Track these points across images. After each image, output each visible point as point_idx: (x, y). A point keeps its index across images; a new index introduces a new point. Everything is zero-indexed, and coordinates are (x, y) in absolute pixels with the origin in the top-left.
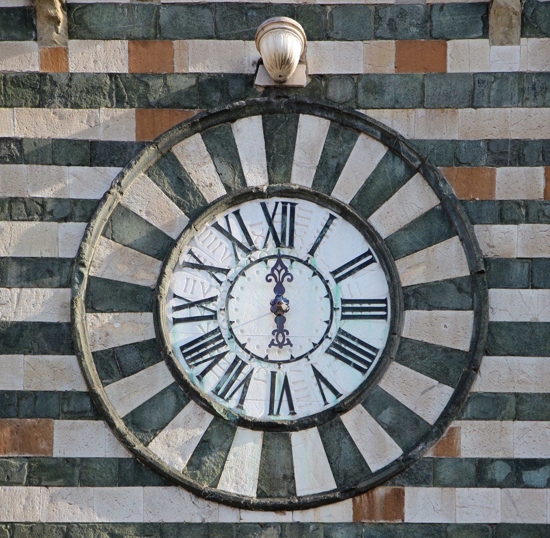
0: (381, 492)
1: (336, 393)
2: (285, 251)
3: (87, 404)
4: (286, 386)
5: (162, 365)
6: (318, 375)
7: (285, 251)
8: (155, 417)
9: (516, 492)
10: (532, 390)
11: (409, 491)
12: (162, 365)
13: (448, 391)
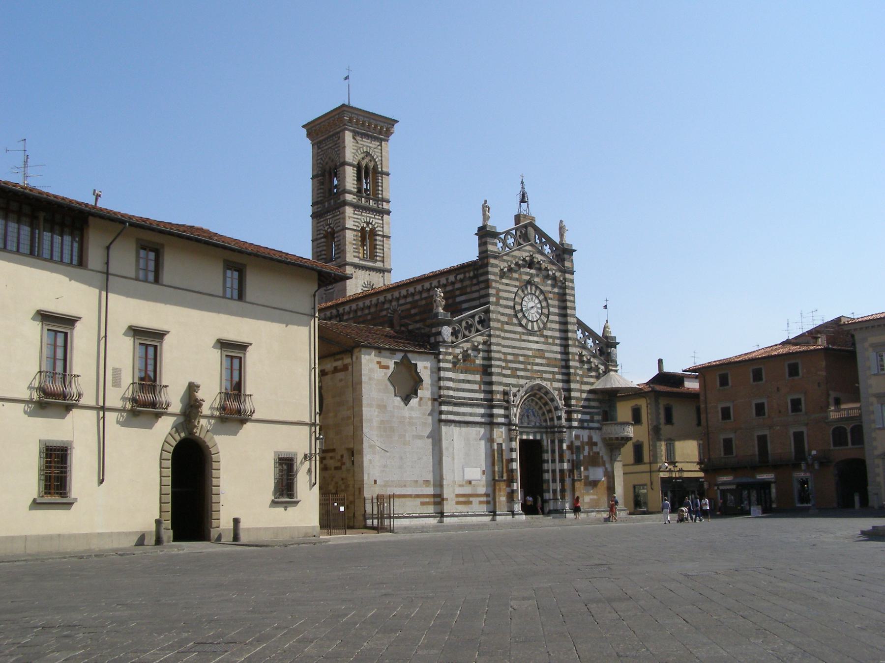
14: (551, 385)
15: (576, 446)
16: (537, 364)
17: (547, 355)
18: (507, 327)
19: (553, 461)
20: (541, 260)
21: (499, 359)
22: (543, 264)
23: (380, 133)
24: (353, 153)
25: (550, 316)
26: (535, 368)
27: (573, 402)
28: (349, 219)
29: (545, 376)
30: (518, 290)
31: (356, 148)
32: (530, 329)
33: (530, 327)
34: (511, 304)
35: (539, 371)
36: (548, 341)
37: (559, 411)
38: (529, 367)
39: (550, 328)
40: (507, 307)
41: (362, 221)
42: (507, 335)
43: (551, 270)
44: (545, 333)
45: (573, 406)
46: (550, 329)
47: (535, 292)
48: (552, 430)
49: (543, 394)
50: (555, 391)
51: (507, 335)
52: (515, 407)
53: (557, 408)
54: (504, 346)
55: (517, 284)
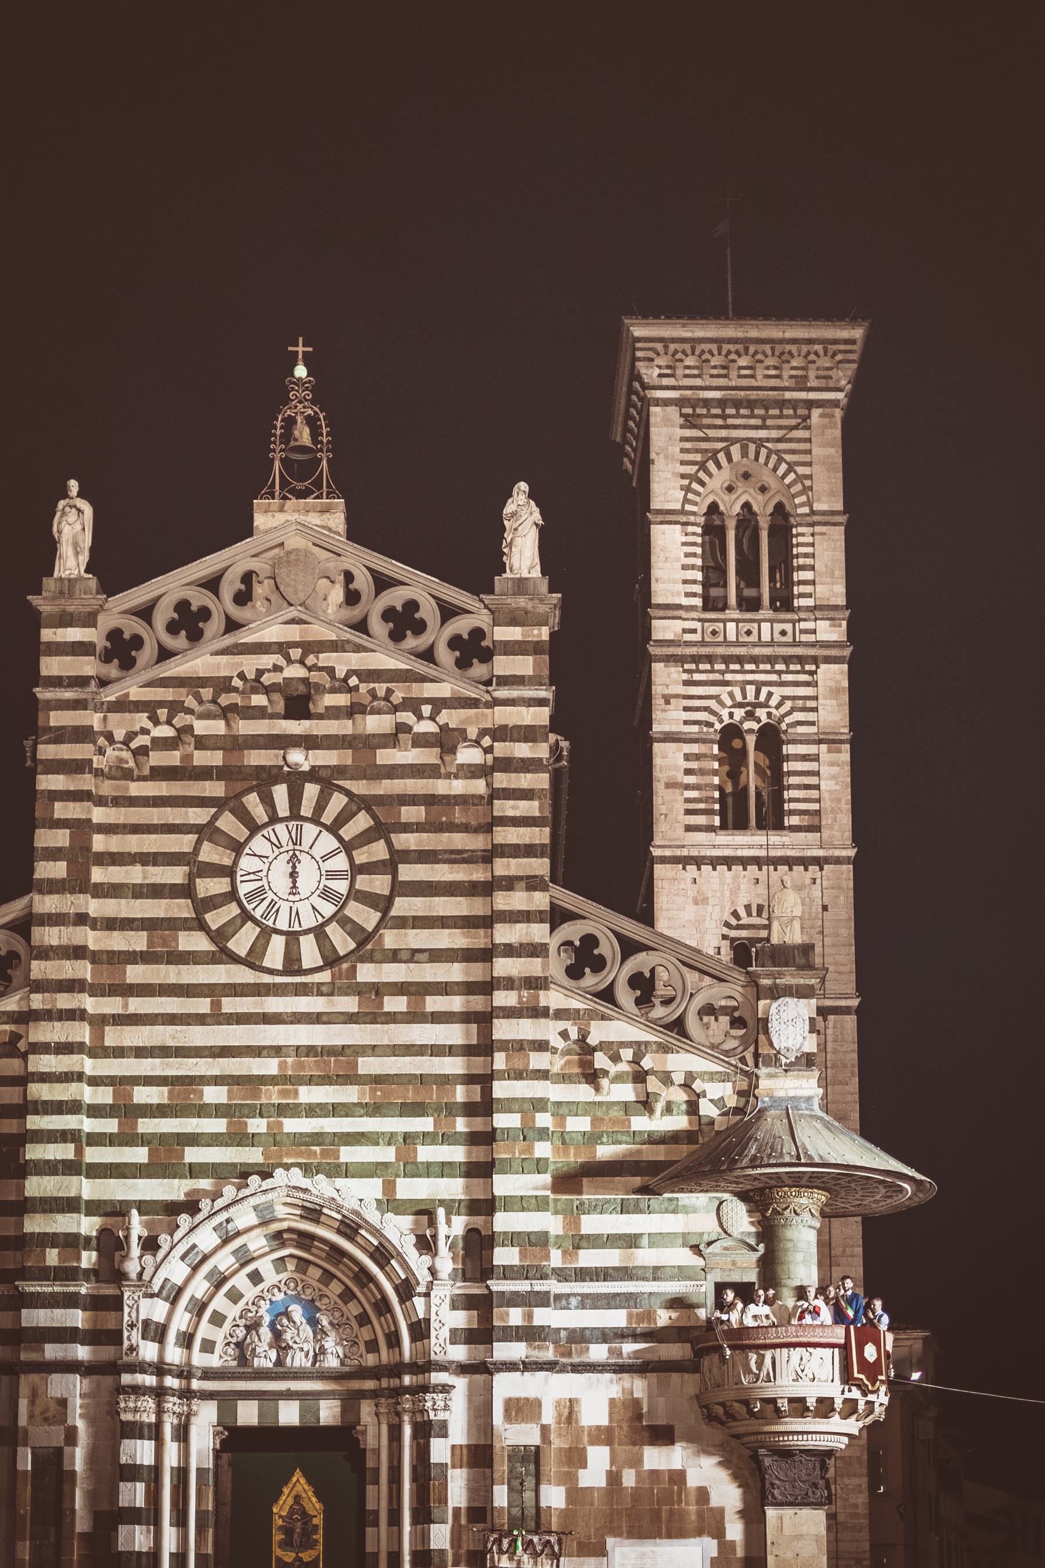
0: (345, 966)
1: (323, 917)
2: (297, 847)
3: (195, 924)
4: (297, 913)
5: (234, 904)
6: (314, 908)
7: (297, 847)
8: (231, 929)
9: (412, 965)
10: (420, 914)
11: (359, 965)
12: (234, 904)
13: (379, 915)
14: (389, 1187)
15: (515, 1448)
16: (313, 1110)
17: (367, 1065)
18: (135, 974)
19: (395, 1519)
20: (350, 673)
21: (74, 1107)
22: (364, 688)
23: (801, 385)
24: (683, 476)
25: (398, 901)
26: (292, 1125)
27: (504, 1256)
28: (667, 702)
29: (348, 1154)
30: (215, 817)
31: (698, 457)
32: (279, 966)
33: (275, 954)
34: (176, 875)
35: (317, 1138)
36: (381, 1004)
37: (416, 1299)
38: (257, 1125)
39: (395, 952)
40: (156, 891)
41: (722, 704)
42: (137, 1005)
43: (413, 705)
44: (366, 973)
45: (508, 1273)
46: (394, 956)
47: (320, 806)
48: (395, 1382)
49: (339, 1232)
50: (389, 1215)
51: (137, 1005)
52: (152, 1296)
53: (406, 1290)
54: (119, 1052)
55: (215, 789)
